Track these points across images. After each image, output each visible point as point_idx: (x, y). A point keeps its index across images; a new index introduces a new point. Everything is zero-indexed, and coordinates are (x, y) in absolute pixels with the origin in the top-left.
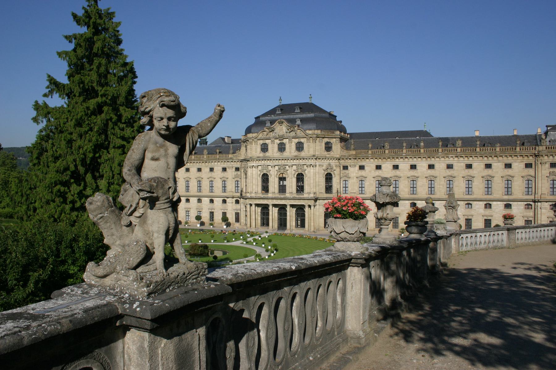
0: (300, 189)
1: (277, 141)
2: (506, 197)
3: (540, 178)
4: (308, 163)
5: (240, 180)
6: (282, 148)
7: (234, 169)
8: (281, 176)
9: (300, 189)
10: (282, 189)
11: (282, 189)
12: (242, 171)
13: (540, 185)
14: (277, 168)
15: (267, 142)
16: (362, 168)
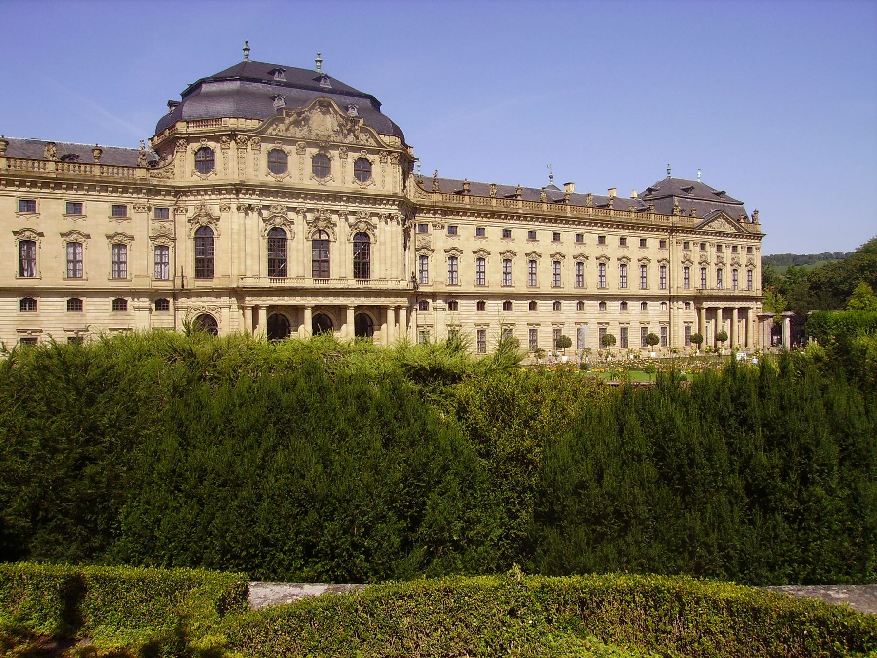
0: (362, 269)
1: (315, 151)
2: (642, 292)
3: (675, 264)
4: (383, 211)
5: (171, 246)
6: (321, 166)
7: (152, 214)
8: (316, 237)
9: (362, 269)
10: (321, 267)
11: (321, 267)
12: (182, 219)
13: (676, 274)
14: (310, 217)
15: (286, 148)
16: (452, 230)
